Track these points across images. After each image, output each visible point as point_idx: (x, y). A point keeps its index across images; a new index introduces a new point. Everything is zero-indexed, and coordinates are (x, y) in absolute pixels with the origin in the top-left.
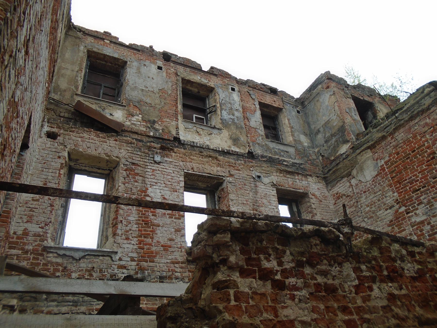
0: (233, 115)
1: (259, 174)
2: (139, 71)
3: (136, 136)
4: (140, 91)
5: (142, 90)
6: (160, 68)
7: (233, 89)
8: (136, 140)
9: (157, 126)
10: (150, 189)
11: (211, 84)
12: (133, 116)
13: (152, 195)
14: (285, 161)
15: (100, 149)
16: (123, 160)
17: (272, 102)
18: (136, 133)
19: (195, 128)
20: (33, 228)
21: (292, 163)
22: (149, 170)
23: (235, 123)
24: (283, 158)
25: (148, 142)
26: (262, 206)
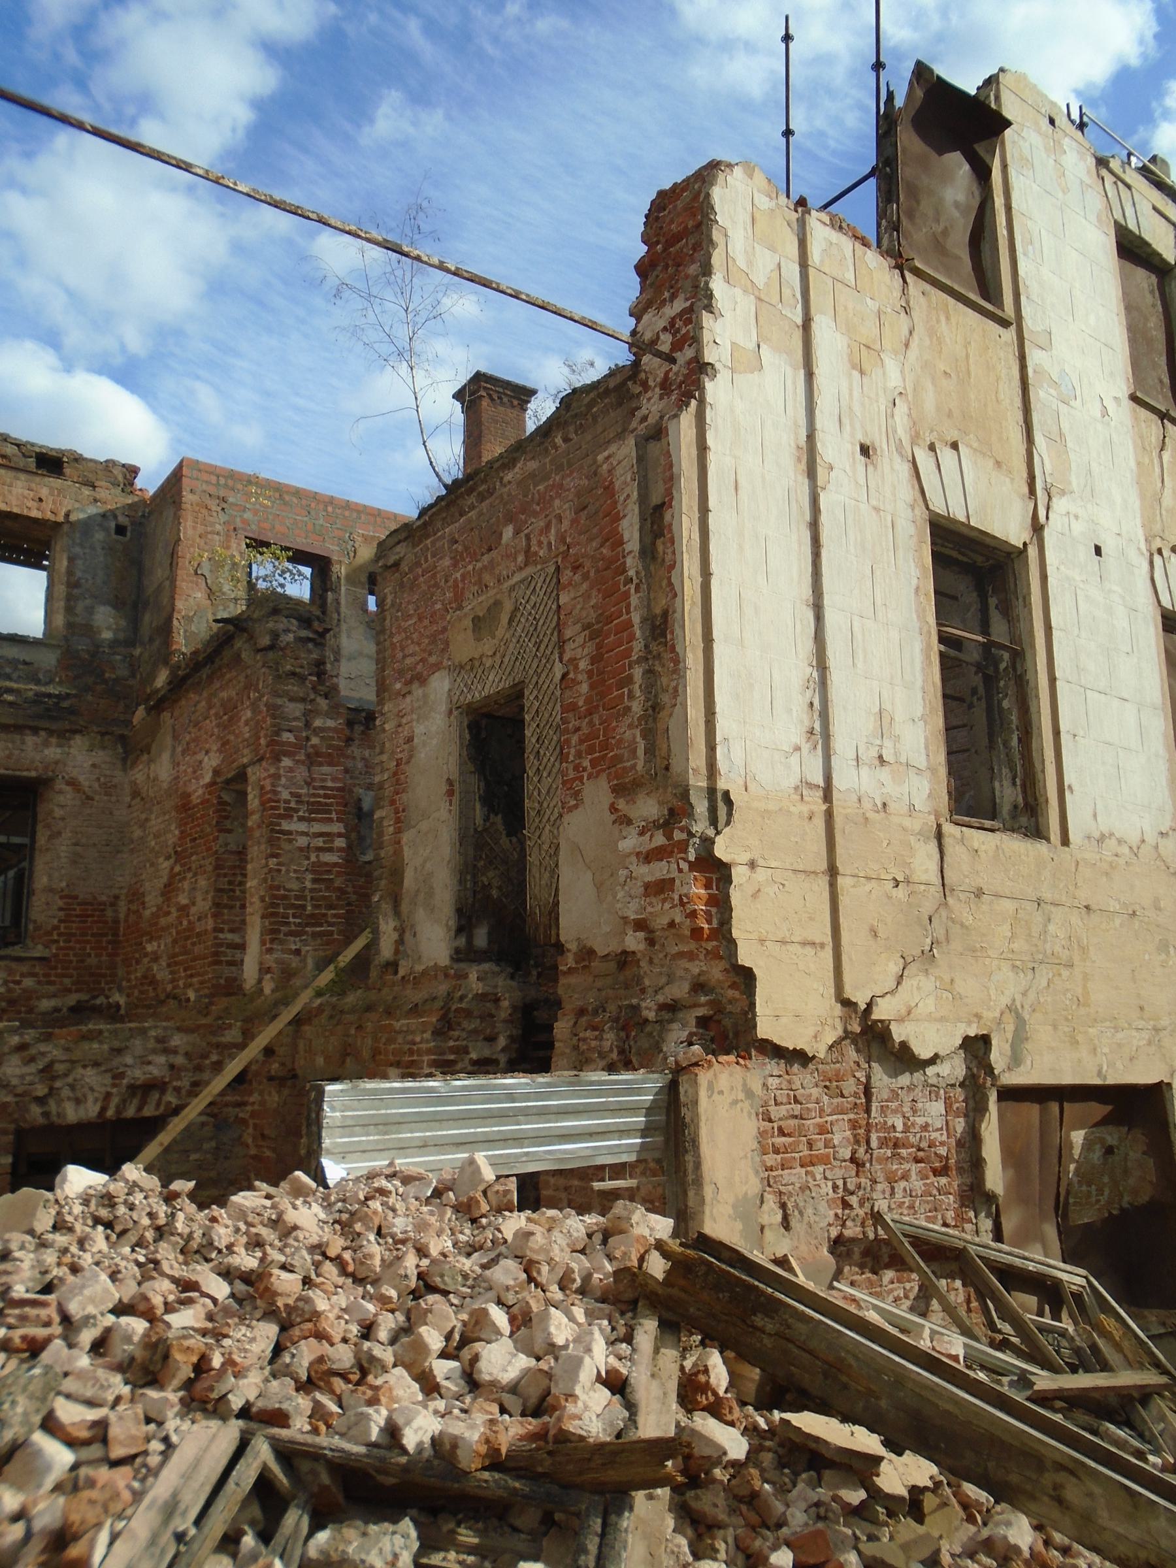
14: (9, 691)
17: (30, 504)
21: (36, 695)
24: (8, 684)
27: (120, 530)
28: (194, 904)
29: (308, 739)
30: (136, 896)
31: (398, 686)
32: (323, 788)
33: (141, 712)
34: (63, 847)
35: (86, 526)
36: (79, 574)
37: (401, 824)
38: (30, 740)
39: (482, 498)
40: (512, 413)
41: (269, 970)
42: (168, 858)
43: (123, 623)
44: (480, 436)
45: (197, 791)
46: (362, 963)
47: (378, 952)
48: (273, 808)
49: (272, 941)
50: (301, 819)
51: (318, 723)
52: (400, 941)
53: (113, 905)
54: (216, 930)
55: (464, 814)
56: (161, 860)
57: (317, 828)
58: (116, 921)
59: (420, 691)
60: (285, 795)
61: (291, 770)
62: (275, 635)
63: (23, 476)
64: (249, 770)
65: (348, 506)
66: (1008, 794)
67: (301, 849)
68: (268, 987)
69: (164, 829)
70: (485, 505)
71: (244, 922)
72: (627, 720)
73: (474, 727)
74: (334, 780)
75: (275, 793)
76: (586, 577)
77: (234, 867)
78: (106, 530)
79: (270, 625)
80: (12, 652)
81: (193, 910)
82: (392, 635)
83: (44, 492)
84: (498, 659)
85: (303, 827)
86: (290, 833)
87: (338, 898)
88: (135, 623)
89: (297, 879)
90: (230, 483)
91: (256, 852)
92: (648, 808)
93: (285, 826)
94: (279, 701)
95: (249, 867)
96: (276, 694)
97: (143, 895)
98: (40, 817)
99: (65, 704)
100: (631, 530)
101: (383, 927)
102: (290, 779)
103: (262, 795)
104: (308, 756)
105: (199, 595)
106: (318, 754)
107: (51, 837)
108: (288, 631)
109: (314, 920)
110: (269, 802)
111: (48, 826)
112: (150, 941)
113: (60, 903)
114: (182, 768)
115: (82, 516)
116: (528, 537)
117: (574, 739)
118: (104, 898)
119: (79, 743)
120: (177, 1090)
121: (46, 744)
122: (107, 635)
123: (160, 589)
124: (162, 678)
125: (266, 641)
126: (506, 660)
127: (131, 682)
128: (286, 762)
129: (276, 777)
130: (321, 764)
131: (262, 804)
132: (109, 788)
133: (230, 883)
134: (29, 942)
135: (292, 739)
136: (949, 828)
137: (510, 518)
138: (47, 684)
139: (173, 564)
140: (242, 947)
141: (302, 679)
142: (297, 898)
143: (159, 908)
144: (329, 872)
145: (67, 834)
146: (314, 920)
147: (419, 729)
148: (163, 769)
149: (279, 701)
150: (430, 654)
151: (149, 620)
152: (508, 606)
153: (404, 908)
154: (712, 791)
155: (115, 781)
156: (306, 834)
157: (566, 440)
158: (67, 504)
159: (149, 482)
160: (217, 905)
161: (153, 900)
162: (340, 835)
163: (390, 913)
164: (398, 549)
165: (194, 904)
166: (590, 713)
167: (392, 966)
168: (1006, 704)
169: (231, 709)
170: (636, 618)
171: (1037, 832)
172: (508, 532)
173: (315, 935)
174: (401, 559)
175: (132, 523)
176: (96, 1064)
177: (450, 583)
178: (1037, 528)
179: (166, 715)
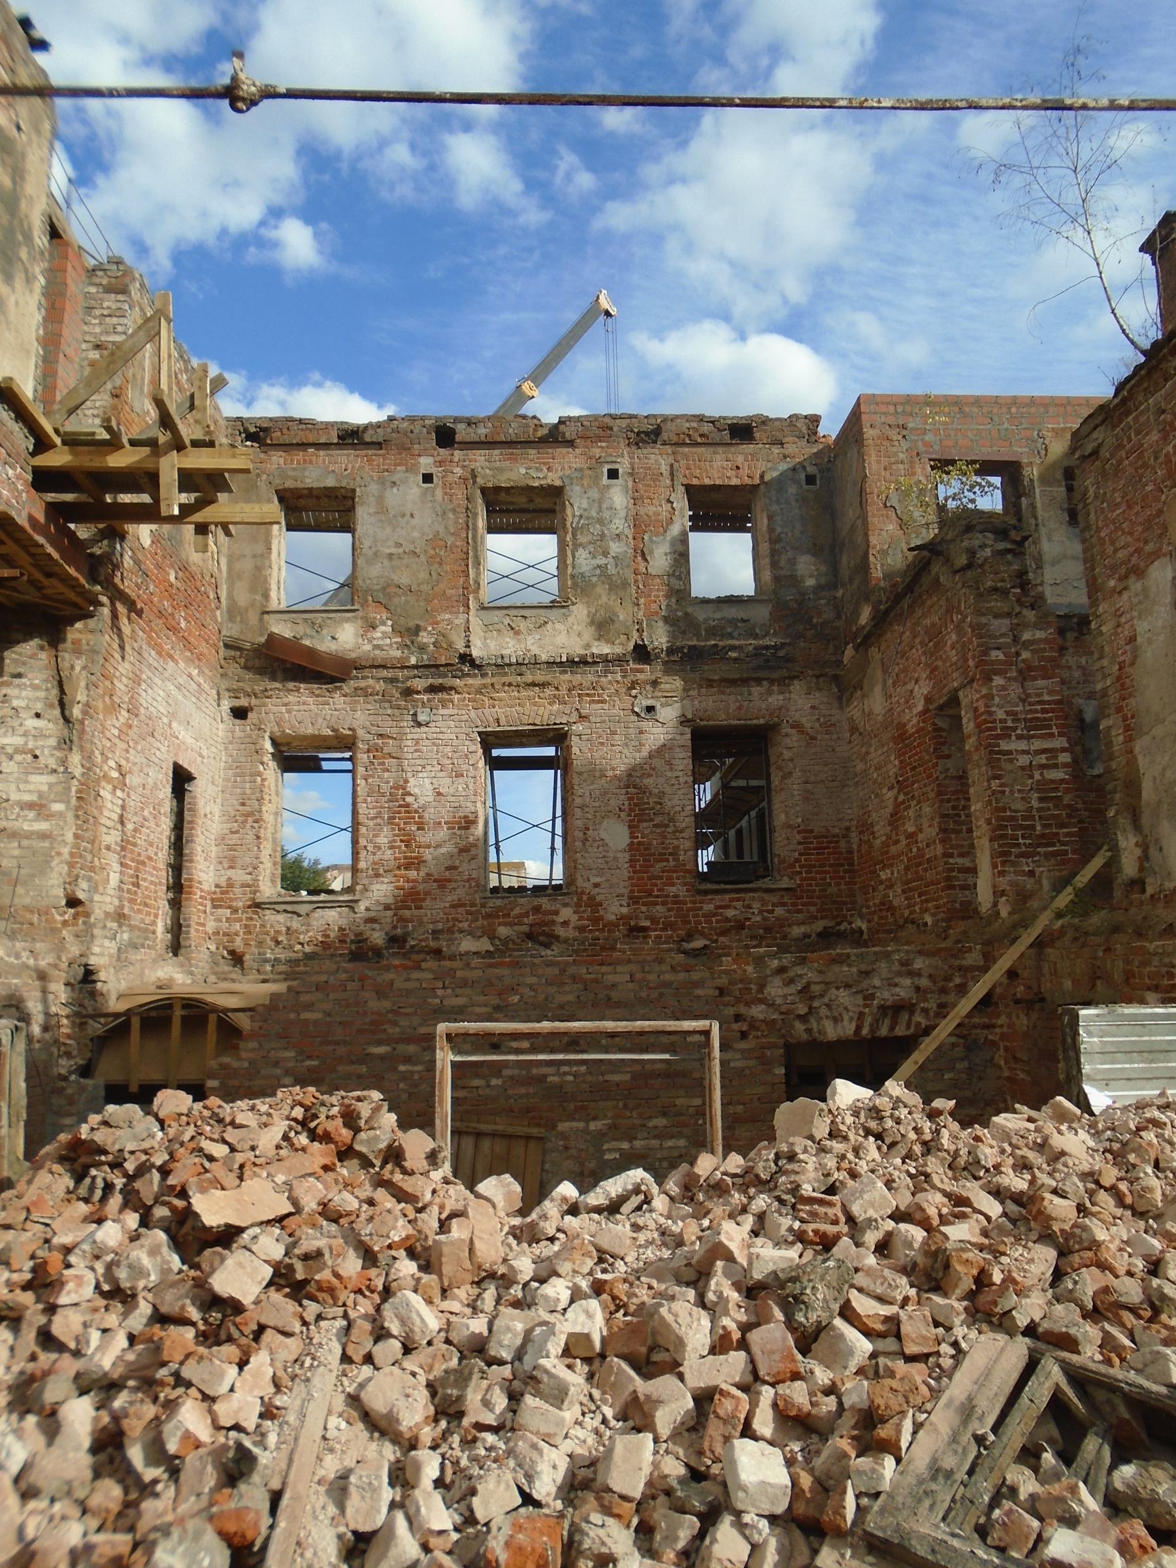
0: (605, 554)
1: (650, 702)
2: (382, 510)
3: (385, 673)
4: (386, 562)
5: (390, 556)
6: (428, 478)
7: (613, 474)
8: (385, 680)
9: (425, 638)
10: (412, 781)
11: (553, 479)
12: (374, 627)
13: (416, 791)
14: (733, 648)
15: (320, 720)
16: (361, 733)
18: (384, 667)
19: (507, 621)
20: (239, 876)
22: (409, 743)
23: (609, 577)
24: (731, 642)
25: (408, 678)
26: (650, 776)
27: (810, 480)
28: (921, 831)
29: (1018, 654)
30: (865, 827)
31: (1112, 583)
32: (1039, 703)
33: (849, 651)
34: (795, 785)
35: (779, 483)
36: (779, 530)
37: (1131, 731)
38: (756, 690)
41: (1003, 893)
42: (891, 788)
43: (823, 568)
45: (911, 719)
46: (1103, 883)
47: (1120, 870)
48: (989, 729)
49: (1004, 863)
50: (1019, 737)
51: (1026, 636)
52: (1145, 857)
53: (844, 836)
54: (947, 855)
56: (885, 791)
57: (1037, 744)
58: (850, 852)
60: (1000, 714)
61: (1004, 688)
62: (972, 553)
63: (720, 450)
64: (961, 693)
65: (1033, 401)
67: (1023, 768)
68: (1004, 912)
69: (884, 760)
71: (972, 846)
74: (1050, 693)
75: (990, 713)
77: (957, 792)
79: (965, 544)
80: (732, 612)
81: (920, 837)
82: (1098, 530)
83: (740, 460)
85: (1022, 745)
86: (1010, 752)
87: (1069, 816)
88: (834, 566)
89: (1022, 799)
90: (908, 409)
91: (977, 775)
93: (1004, 745)
94: (984, 620)
95: (972, 790)
96: (979, 613)
97: (872, 825)
98: (772, 760)
99: (781, 653)
101: (1122, 843)
102: (1004, 697)
103: (976, 717)
104: (1020, 671)
105: (891, 527)
106: (1030, 668)
107: (783, 778)
108: (983, 546)
109: (1047, 839)
110: (984, 724)
111: (780, 768)
112: (883, 869)
113: (799, 838)
114: (894, 700)
115: (775, 474)
118: (837, 831)
119: (797, 686)
120: (925, 1011)
121: (770, 693)
122: (810, 582)
123: (853, 528)
124: (865, 615)
125: (963, 560)
127: (837, 624)
128: (998, 681)
129: (990, 697)
130: (1035, 679)
131: (978, 726)
133: (954, 808)
134: (775, 874)
135: (1001, 657)
138: (764, 637)
139: (862, 503)
140: (974, 871)
141: (1004, 593)
142: (1024, 818)
143: (889, 837)
144: (1057, 789)
145: (797, 773)
146: (1047, 839)
147: (1142, 627)
148: (875, 702)
149: (984, 620)
150: (1146, 542)
151: (847, 562)
153: (1145, 820)
155: (833, 719)
156: (1026, 752)
158: (761, 466)
159: (830, 429)
160: (944, 831)
161: (881, 830)
162: (1063, 750)
163: (1129, 827)
164: (1095, 435)
165: (921, 831)
167: (1138, 884)
169: (935, 635)
173: (1047, 856)
174: (1100, 445)
176: (847, 986)
177: (1162, 459)
179: (873, 650)
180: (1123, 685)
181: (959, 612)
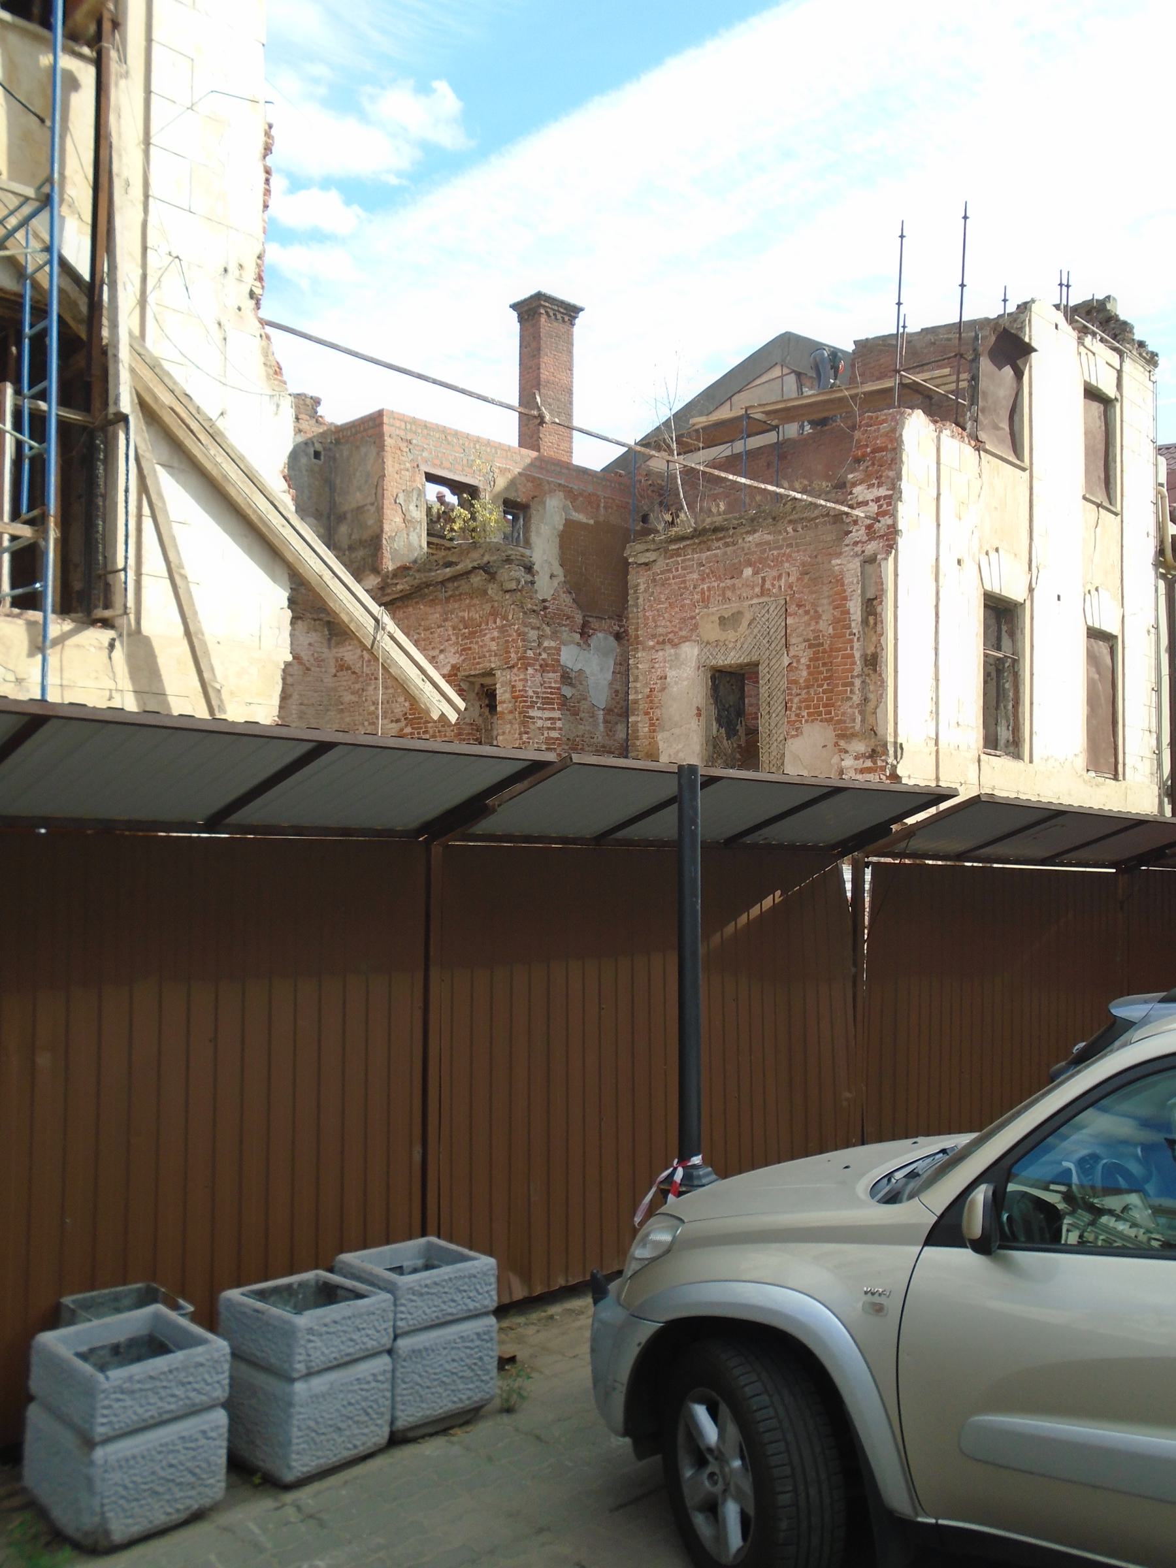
31: (651, 643)
32: (550, 688)
37: (654, 727)
39: (727, 545)
40: (563, 328)
44: (539, 349)
50: (539, 708)
51: (546, 644)
55: (708, 728)
57: (547, 714)
59: (672, 651)
60: (530, 693)
65: (488, 443)
66: (1004, 734)
67: (539, 729)
70: (729, 549)
72: (849, 704)
73: (713, 678)
74: (555, 682)
76: (807, 612)
77: (469, 734)
78: (307, 455)
84: (739, 645)
86: (532, 718)
92: (860, 747)
93: (534, 713)
94: (526, 630)
96: (525, 624)
100: (855, 608)
102: (532, 682)
103: (513, 692)
110: (517, 696)
116: (764, 579)
117: (796, 700)
126: (745, 646)
128: (530, 671)
129: (526, 680)
132: (320, 661)
136: (983, 757)
137: (749, 564)
145: (296, 696)
147: (671, 674)
149: (526, 630)
150: (681, 629)
152: (748, 616)
154: (895, 743)
155: (324, 656)
156: (541, 718)
157: (795, 530)
162: (560, 719)
166: (808, 687)
168: (1007, 686)
170: (857, 655)
171: (1018, 756)
172: (748, 572)
175: (324, 449)
177: (699, 589)
178: (1031, 590)
180: (651, 702)
181: (505, 618)
